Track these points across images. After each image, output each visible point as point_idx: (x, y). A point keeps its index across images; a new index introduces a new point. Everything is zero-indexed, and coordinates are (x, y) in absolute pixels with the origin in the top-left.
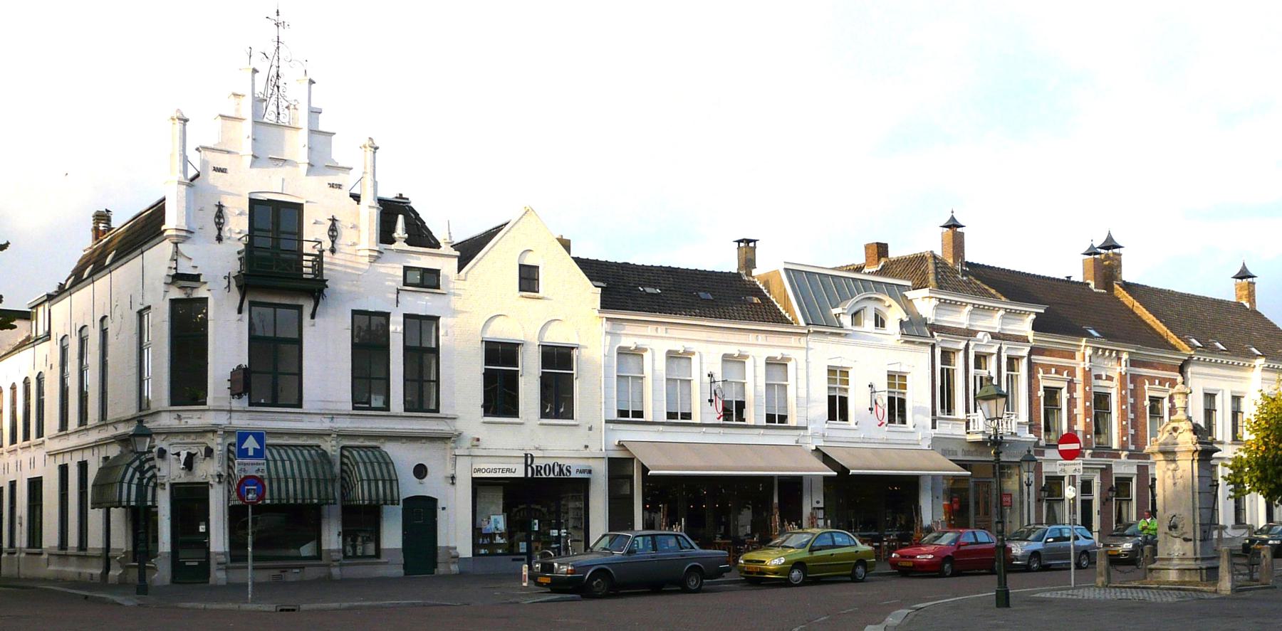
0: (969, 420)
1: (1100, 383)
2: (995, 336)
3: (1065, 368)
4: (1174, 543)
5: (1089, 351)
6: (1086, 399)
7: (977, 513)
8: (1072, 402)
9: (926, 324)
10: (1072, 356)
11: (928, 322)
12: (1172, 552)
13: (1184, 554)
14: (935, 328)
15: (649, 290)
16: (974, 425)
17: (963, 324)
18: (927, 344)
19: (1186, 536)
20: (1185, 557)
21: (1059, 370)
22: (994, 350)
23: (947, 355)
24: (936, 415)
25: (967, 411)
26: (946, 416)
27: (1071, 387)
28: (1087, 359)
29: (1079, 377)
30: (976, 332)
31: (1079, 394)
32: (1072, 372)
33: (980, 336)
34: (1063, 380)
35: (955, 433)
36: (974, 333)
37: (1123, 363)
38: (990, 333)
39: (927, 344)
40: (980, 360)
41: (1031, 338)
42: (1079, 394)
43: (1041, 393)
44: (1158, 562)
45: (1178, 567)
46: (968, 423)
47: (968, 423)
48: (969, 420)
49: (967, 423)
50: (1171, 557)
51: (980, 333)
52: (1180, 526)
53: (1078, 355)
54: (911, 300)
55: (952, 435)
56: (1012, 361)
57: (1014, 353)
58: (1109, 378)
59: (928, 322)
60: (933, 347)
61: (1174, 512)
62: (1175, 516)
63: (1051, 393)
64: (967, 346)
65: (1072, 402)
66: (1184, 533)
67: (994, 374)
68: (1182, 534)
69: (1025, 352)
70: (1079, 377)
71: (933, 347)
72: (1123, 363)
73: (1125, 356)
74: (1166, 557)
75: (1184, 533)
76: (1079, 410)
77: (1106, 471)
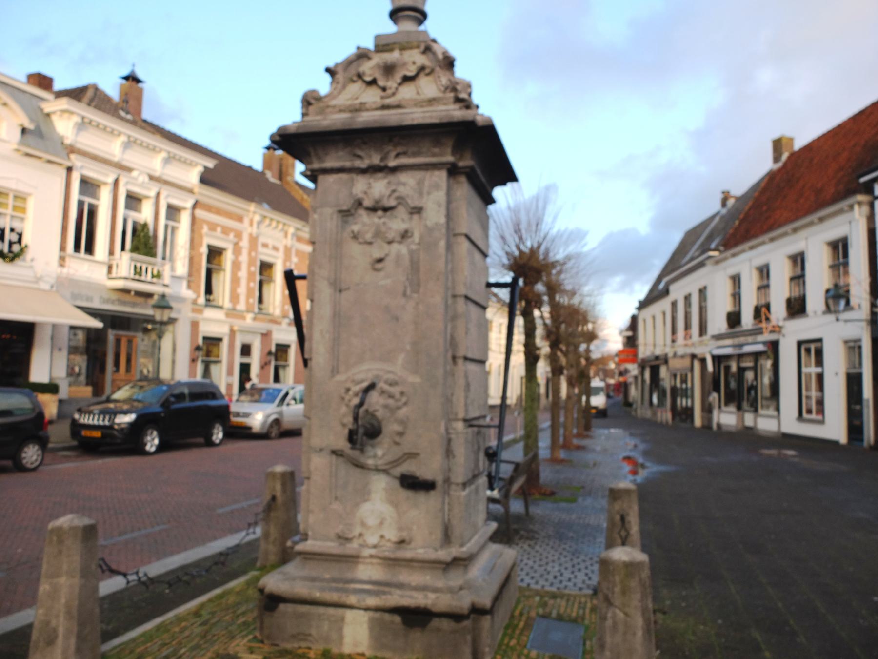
1: (265, 250)
3: (232, 230)
4: (364, 495)
5: (257, 218)
6: (251, 263)
8: (236, 265)
10: (240, 219)
12: (357, 530)
13: (402, 542)
14: (71, 150)
17: (114, 156)
19: (408, 467)
20: (408, 554)
21: (226, 231)
22: (153, 194)
23: (88, 186)
27: (237, 251)
28: (255, 225)
29: (245, 243)
31: (244, 258)
32: (239, 235)
34: (229, 241)
37: (289, 236)
40: (133, 200)
41: (196, 190)
42: (244, 258)
43: (204, 251)
44: (291, 568)
45: (372, 601)
50: (352, 548)
52: (390, 428)
53: (246, 221)
54: (48, 115)
56: (173, 211)
57: (175, 202)
58: (275, 249)
60: (69, 170)
61: (364, 372)
62: (371, 387)
63: (215, 253)
65: (236, 265)
66: (412, 456)
67: (150, 220)
68: (396, 463)
69: (189, 204)
70: (245, 243)
71: (69, 170)
72: (289, 236)
73: (291, 230)
74: (331, 547)
75: (412, 456)
76: (243, 274)
77: (266, 336)
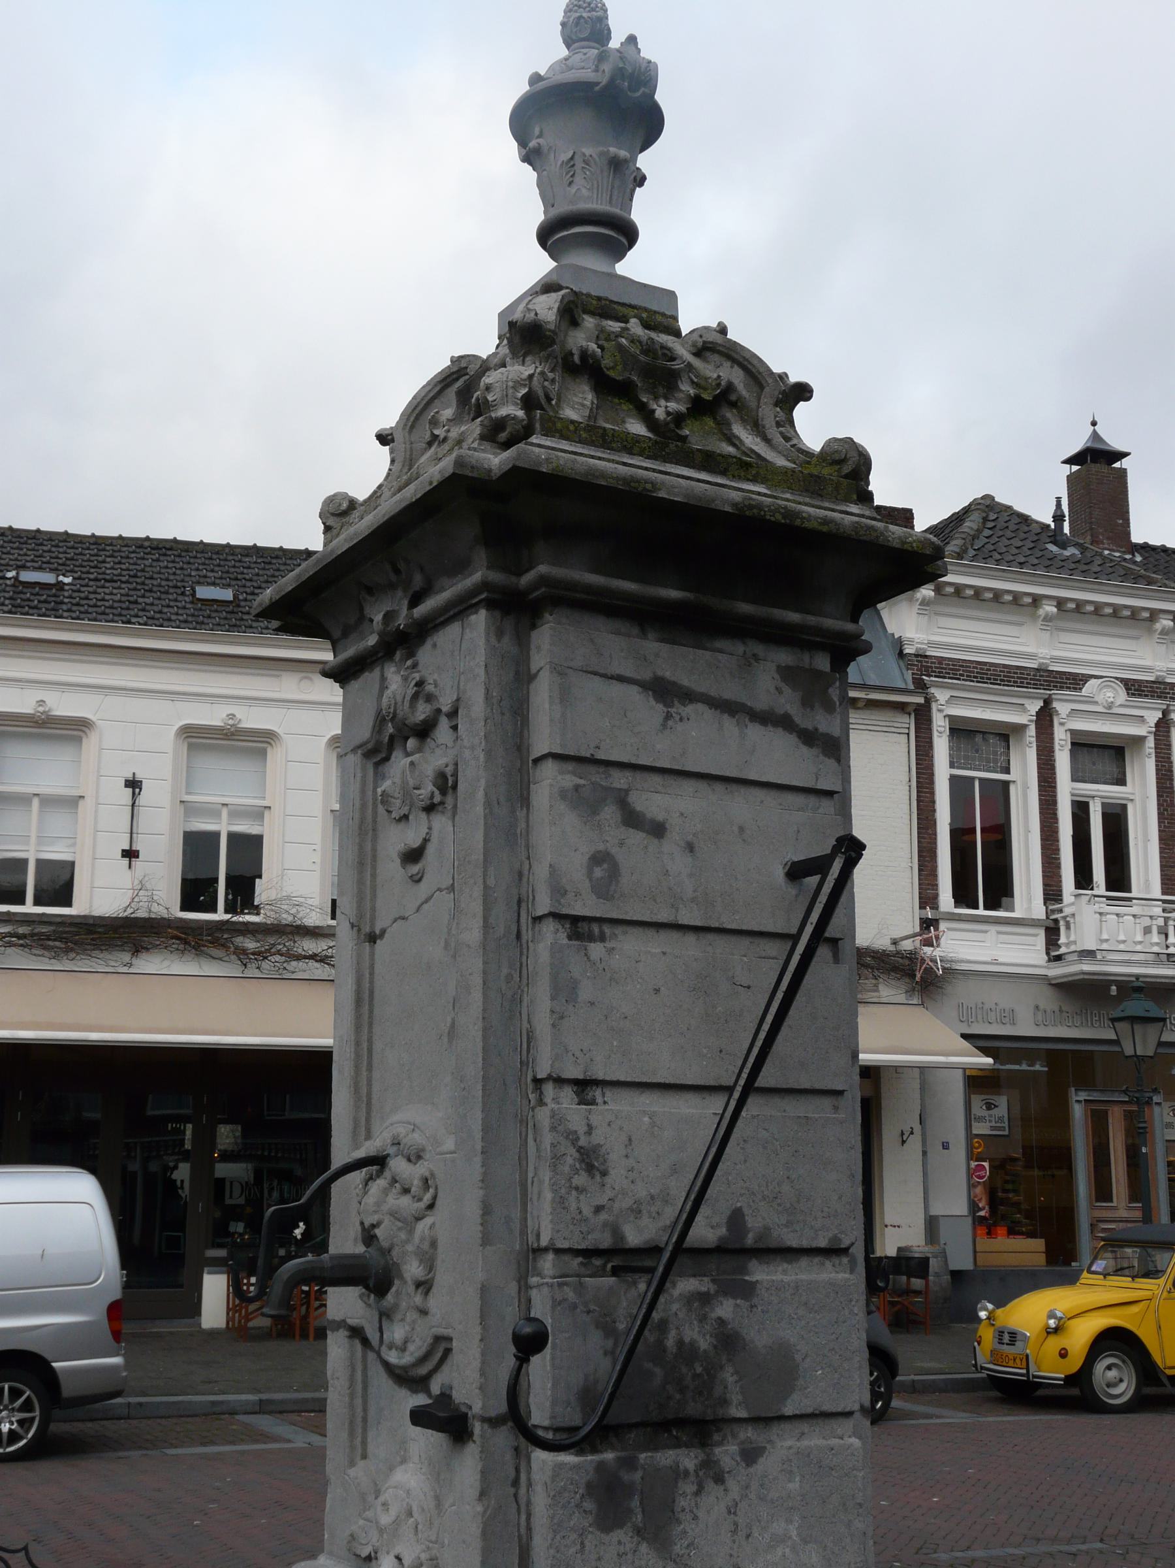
0: (1056, 921)
2: (1134, 688)
7: (1103, 1192)
9: (901, 654)
11: (907, 651)
15: (27, 576)
16: (1068, 937)
18: (901, 707)
24: (935, 907)
25: (1052, 894)
26: (981, 911)
30: (1085, 678)
33: (1090, 687)
35: (1001, 960)
36: (1076, 682)
38: (1122, 680)
39: (901, 707)
46: (1052, 933)
47: (1052, 933)
48: (1056, 921)
49: (1048, 930)
51: (1092, 682)
55: (995, 962)
59: (907, 651)
64: (1045, 717)
